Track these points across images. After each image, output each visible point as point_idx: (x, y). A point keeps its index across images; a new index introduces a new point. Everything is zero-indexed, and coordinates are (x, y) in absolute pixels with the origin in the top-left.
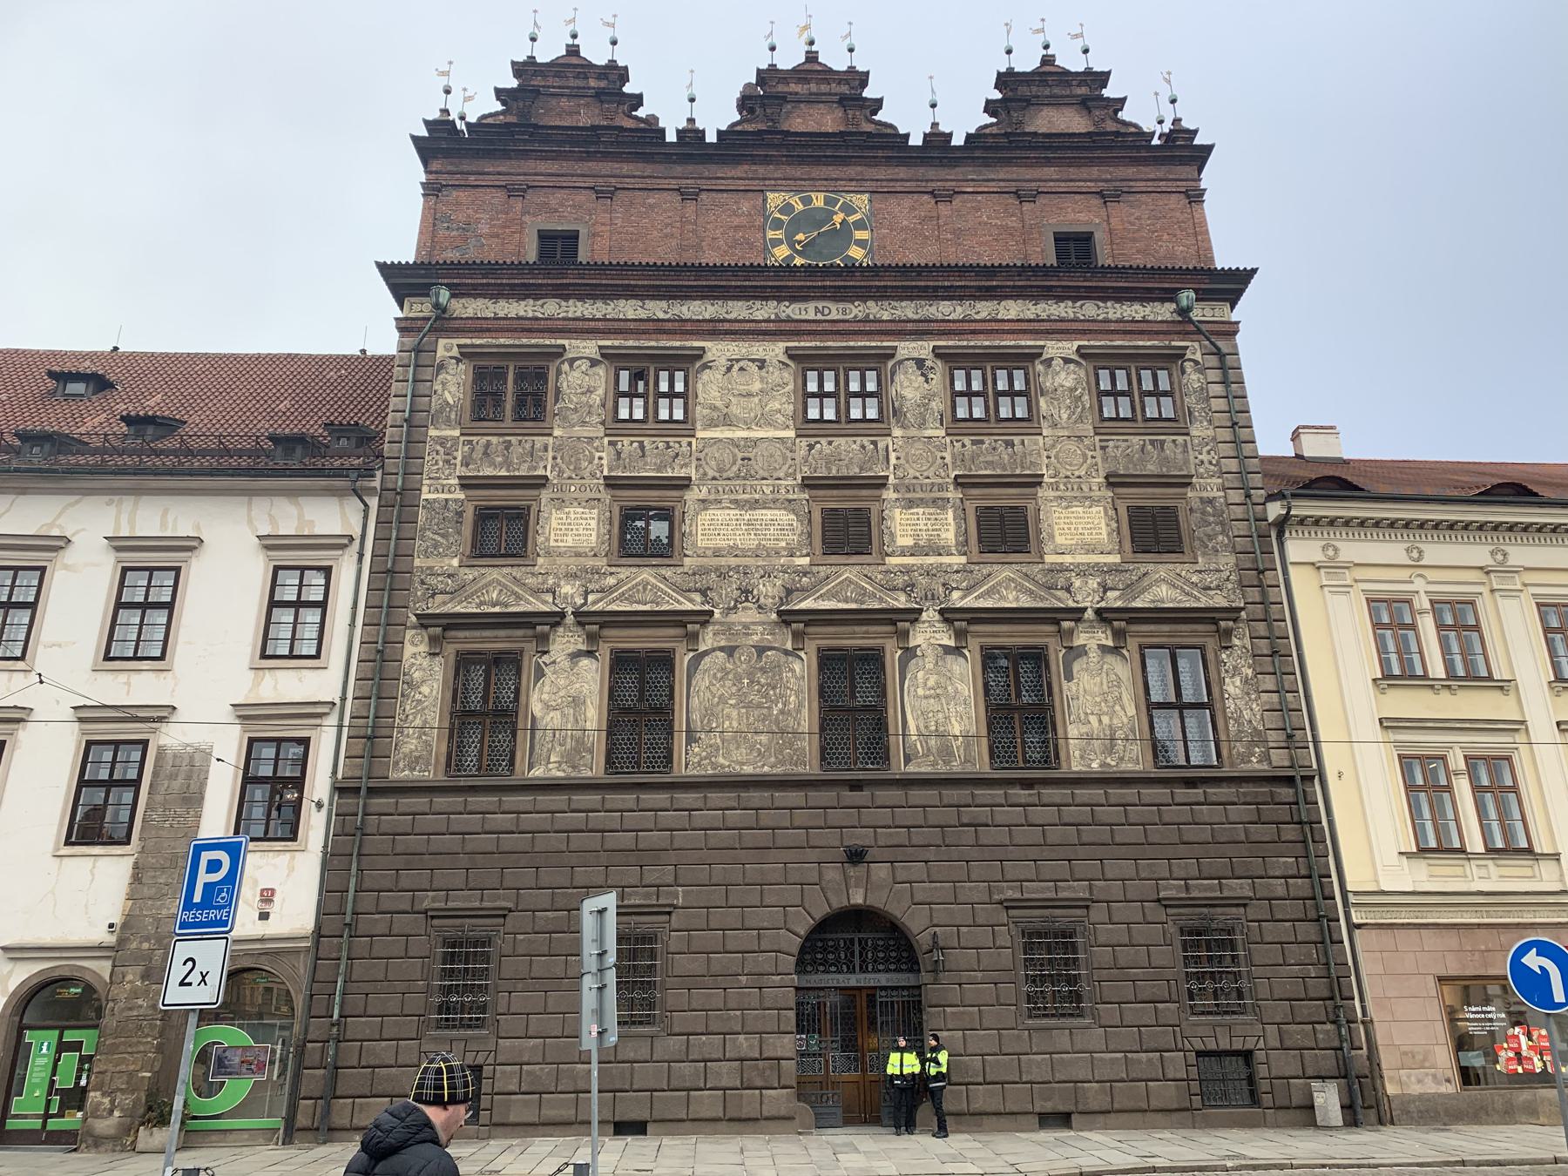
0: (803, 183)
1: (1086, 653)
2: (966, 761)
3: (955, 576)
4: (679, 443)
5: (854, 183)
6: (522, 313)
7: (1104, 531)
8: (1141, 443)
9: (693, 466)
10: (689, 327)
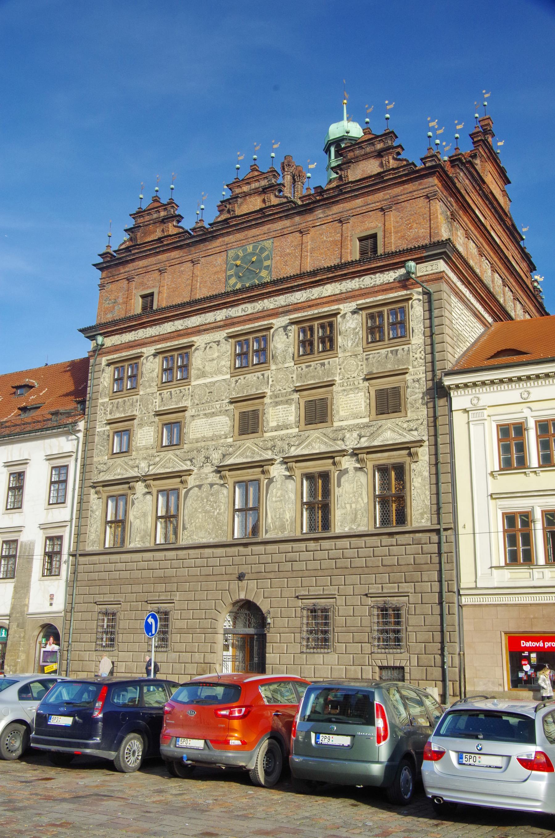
0: (244, 241)
1: (348, 472)
2: (291, 531)
3: (294, 439)
4: (185, 389)
5: (265, 235)
6: (130, 339)
7: (363, 406)
8: (386, 353)
9: (190, 399)
10: (189, 331)
